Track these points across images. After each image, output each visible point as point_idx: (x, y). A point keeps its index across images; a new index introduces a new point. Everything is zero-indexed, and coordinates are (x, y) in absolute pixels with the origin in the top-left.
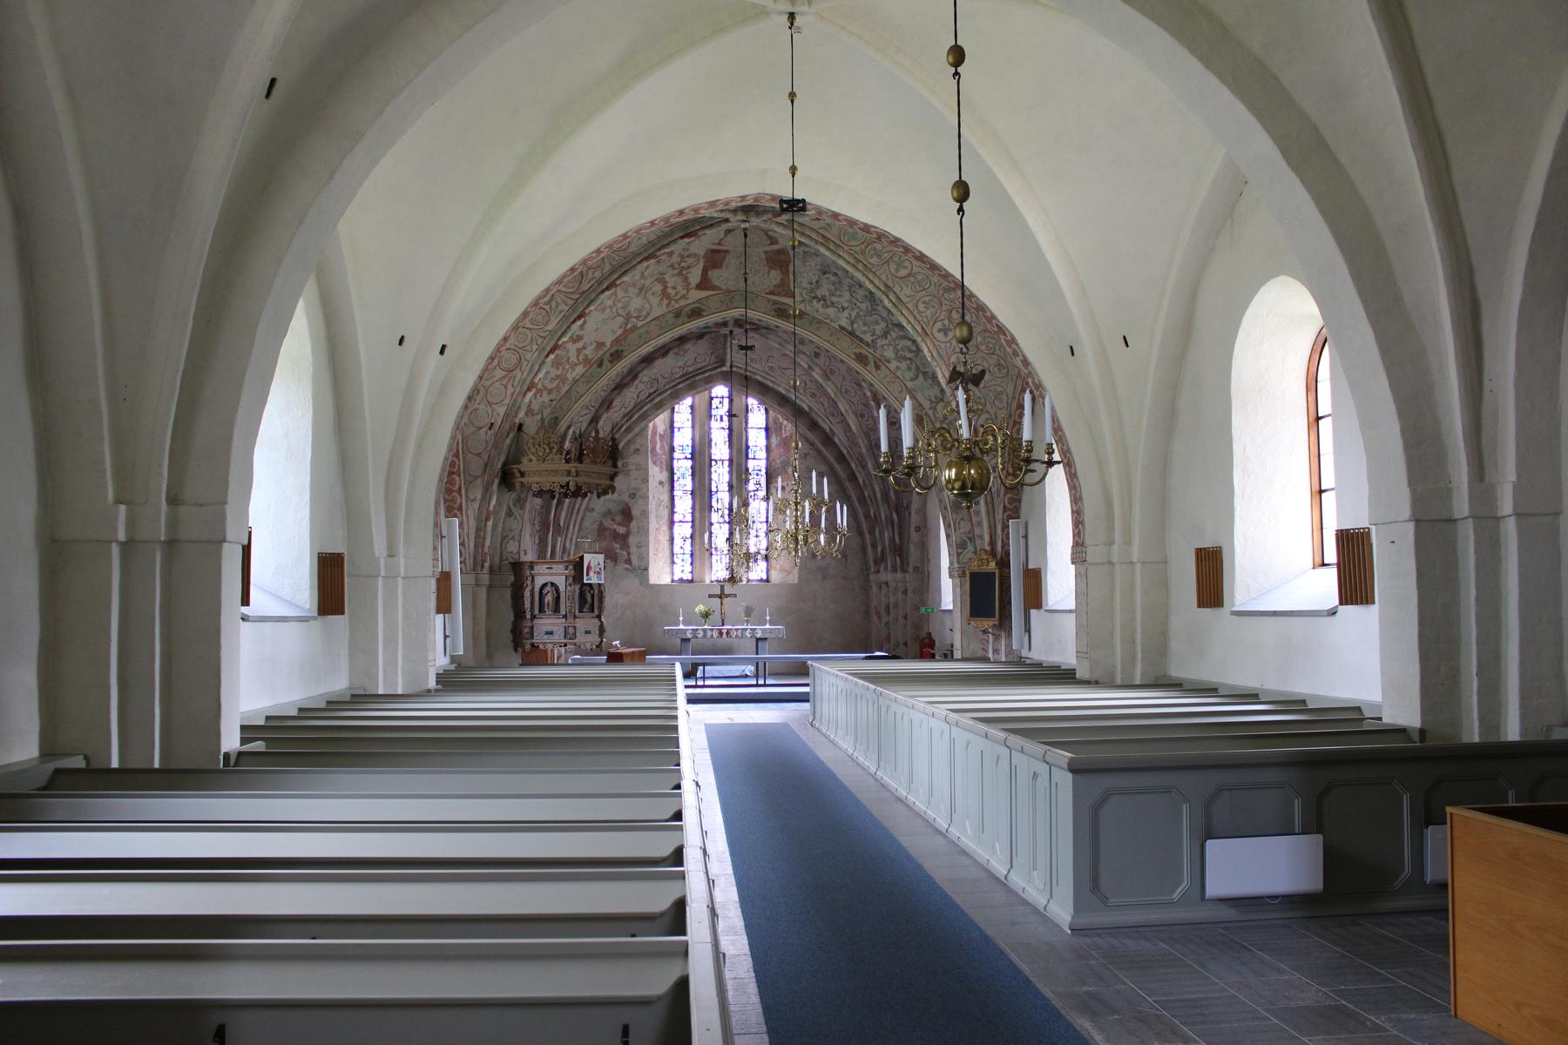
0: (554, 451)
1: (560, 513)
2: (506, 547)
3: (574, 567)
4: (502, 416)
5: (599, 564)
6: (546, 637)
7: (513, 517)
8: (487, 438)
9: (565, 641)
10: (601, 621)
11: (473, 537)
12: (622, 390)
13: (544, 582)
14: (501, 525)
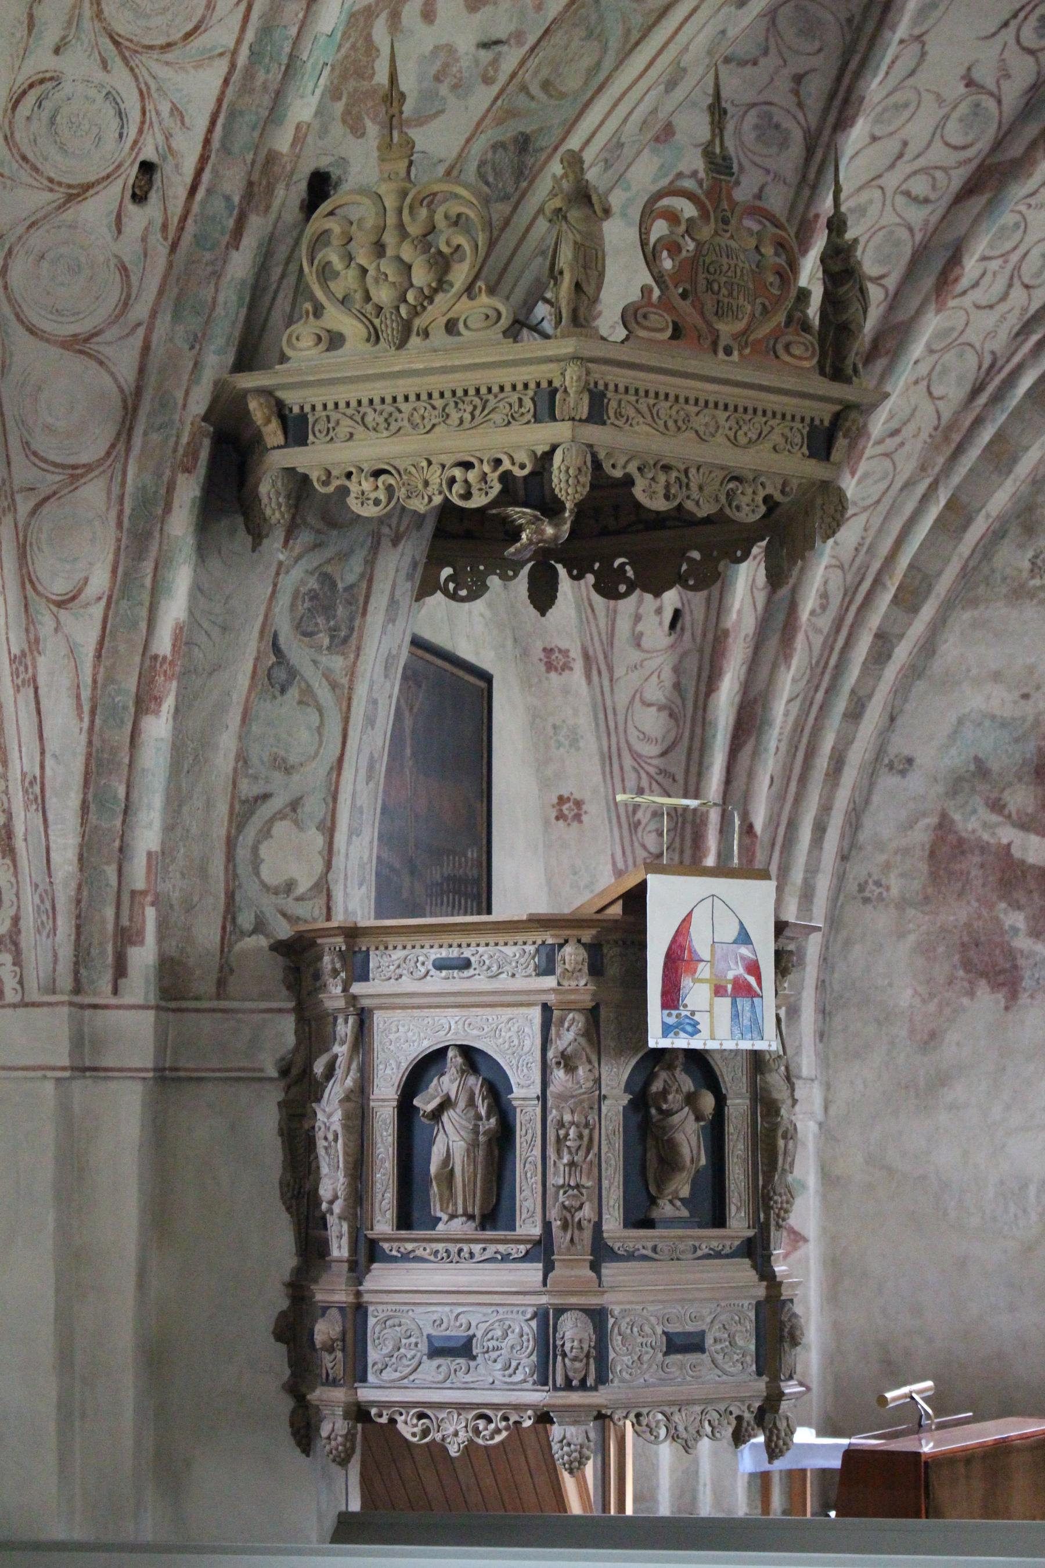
0: (460, 274)
1: (751, 775)
2: (256, 863)
3: (594, 950)
4: (201, 124)
5: (744, 937)
6: (431, 1370)
7: (293, 693)
8: (128, 248)
9: (538, 1397)
10: (767, 1275)
11: (74, 800)
12: (1001, 186)
13: (427, 1045)
14: (227, 742)
